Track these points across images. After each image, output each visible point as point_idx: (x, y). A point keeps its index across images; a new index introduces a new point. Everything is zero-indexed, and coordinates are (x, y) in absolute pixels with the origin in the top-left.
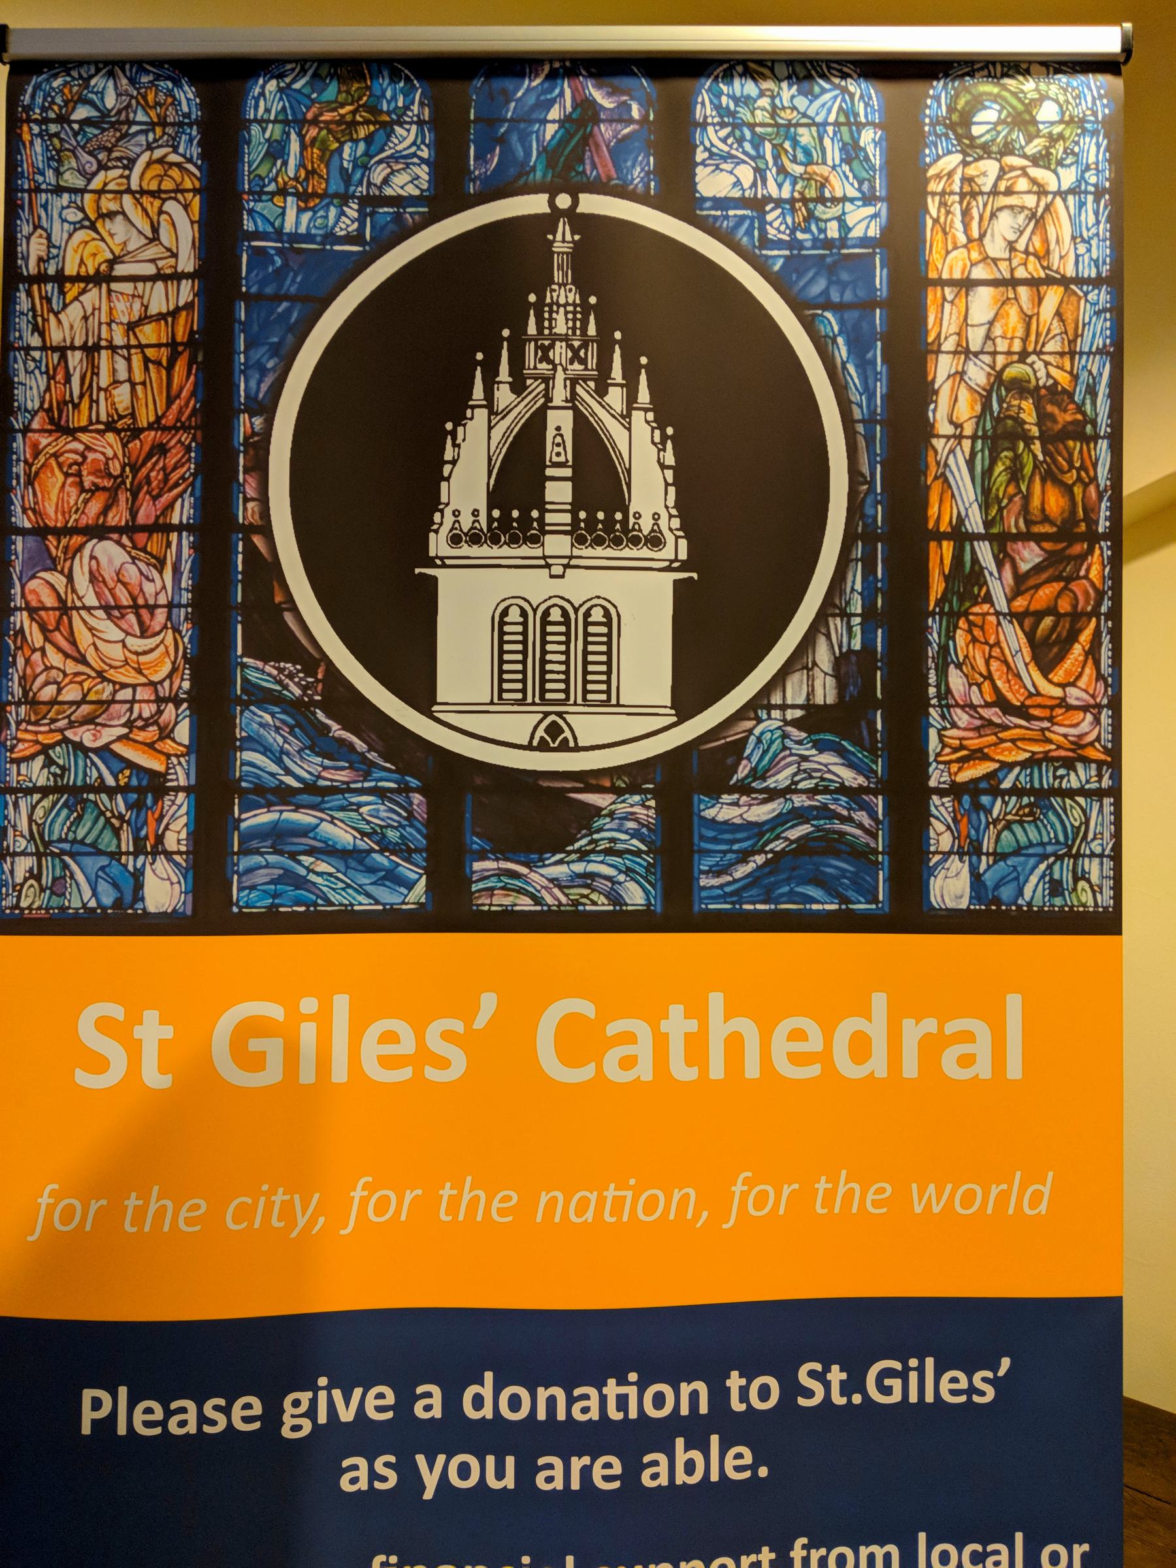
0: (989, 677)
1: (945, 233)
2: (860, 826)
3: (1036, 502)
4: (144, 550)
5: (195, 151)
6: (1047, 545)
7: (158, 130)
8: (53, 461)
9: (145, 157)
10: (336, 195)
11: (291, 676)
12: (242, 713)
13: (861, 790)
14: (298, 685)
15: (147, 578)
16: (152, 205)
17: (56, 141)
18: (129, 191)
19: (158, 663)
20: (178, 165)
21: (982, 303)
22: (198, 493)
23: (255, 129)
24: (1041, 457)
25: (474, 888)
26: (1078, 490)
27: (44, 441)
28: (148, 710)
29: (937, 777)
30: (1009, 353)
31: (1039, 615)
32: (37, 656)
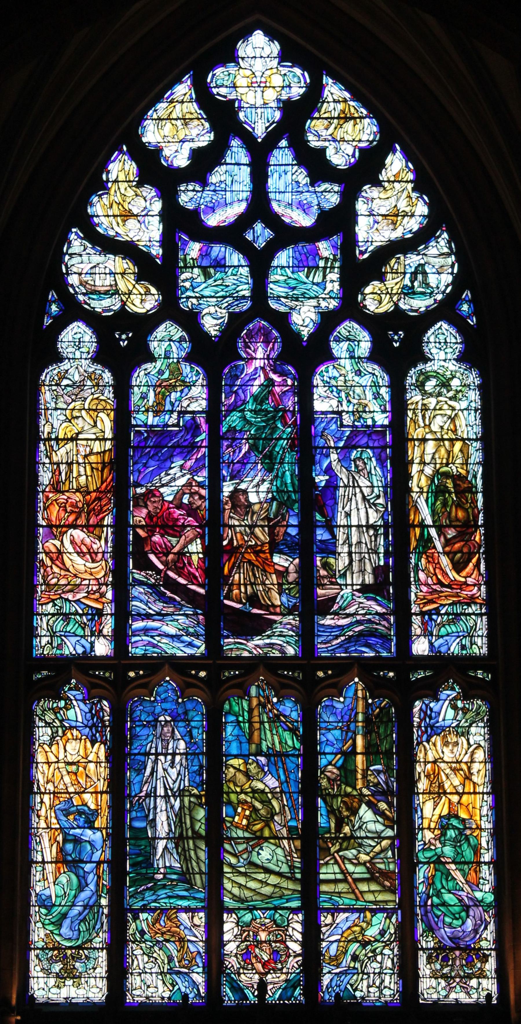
0: (435, 574)
1: (415, 423)
2: (384, 626)
3: (453, 514)
4: (93, 533)
5: (111, 396)
6: (458, 529)
7: (96, 388)
8: (54, 503)
9: (91, 397)
10: (168, 411)
11: (151, 576)
13: (384, 613)
16: (94, 414)
17: (55, 392)
18: (84, 409)
19: (98, 573)
20: (104, 400)
21: (430, 447)
22: (114, 514)
23: (136, 389)
24: (455, 499)
25: (225, 648)
27: (51, 495)
28: (95, 588)
29: (415, 609)
30: (441, 463)
31: (455, 553)
32: (49, 569)
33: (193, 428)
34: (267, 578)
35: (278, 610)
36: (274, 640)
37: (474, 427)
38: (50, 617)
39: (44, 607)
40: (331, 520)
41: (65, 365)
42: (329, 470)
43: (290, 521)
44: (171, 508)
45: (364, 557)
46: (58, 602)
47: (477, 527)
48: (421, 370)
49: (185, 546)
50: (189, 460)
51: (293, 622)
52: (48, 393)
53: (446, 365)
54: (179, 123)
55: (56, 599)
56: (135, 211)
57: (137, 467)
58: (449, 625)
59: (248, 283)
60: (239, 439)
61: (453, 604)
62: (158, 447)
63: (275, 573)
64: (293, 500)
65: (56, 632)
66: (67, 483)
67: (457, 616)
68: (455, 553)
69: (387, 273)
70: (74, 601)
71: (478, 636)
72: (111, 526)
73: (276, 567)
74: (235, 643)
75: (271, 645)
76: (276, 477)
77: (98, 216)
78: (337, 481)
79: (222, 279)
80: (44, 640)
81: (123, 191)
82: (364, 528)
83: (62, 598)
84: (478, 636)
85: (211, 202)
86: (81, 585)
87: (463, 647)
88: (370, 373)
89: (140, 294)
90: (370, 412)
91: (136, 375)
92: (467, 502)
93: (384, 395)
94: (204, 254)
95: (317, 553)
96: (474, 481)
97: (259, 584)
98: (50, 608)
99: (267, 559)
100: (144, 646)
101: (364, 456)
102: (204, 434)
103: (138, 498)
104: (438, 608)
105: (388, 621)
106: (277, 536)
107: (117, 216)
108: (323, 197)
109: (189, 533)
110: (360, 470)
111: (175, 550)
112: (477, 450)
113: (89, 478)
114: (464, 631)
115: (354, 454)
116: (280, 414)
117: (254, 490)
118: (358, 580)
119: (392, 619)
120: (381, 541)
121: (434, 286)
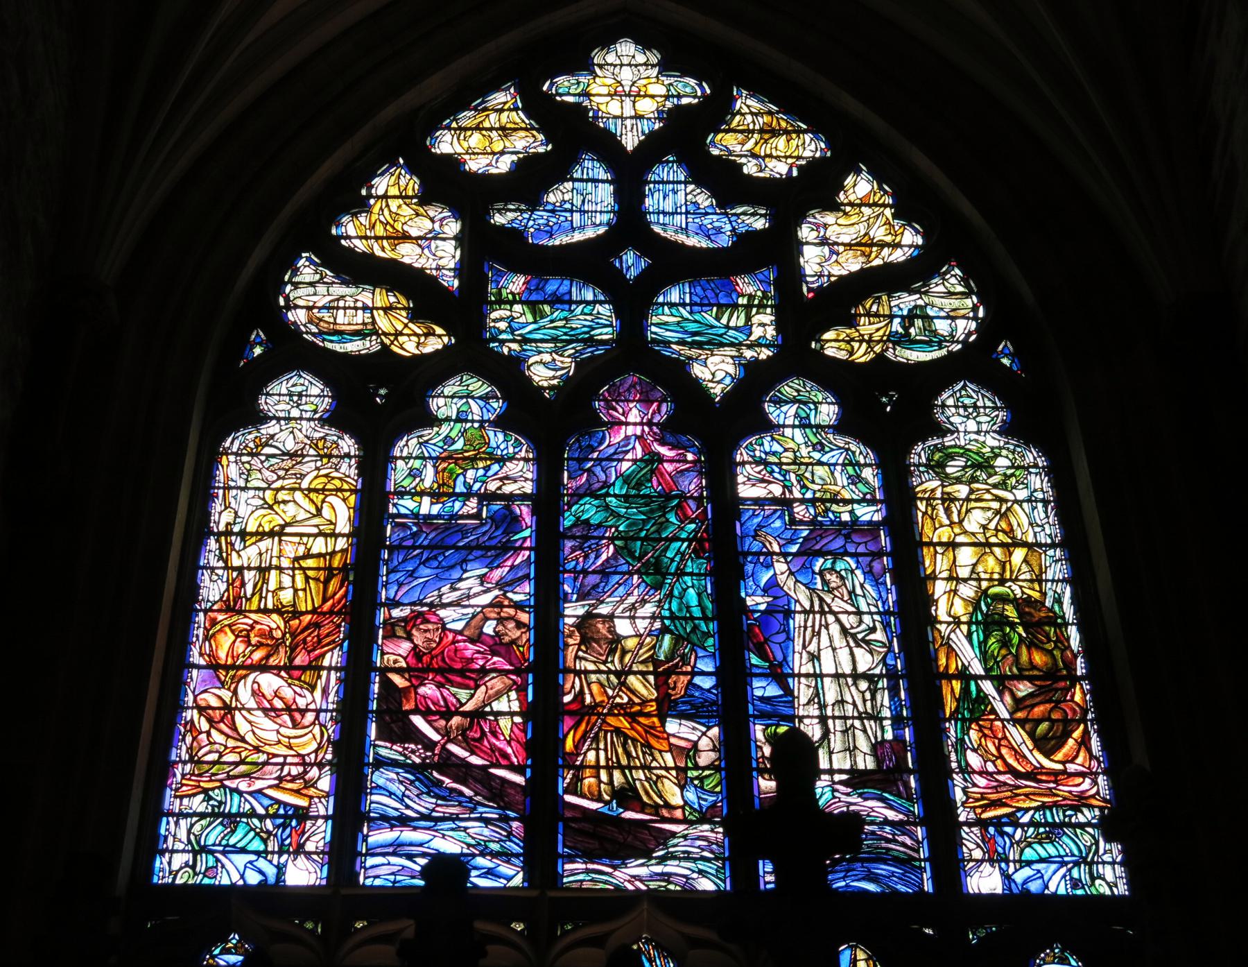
0: (1001, 757)
4: (299, 679)
5: (353, 472)
6: (1038, 683)
8: (227, 629)
11: (413, 752)
12: (372, 773)
13: (901, 823)
14: (419, 757)
15: (300, 695)
16: (318, 498)
17: (247, 466)
18: (300, 489)
20: (340, 479)
21: (966, 556)
22: (345, 648)
23: (400, 463)
24: (1024, 635)
25: (565, 880)
26: (1057, 653)
28: (295, 771)
30: (991, 580)
32: (203, 736)
34: (654, 759)
35: (678, 814)
36: (672, 867)
37: (1047, 526)
38: (195, 819)
39: (185, 801)
40: (781, 665)
41: (271, 428)
42: (772, 586)
43: (698, 665)
44: (459, 641)
45: (852, 725)
46: (217, 794)
47: (1075, 680)
48: (935, 446)
50: (497, 567)
52: (233, 466)
53: (981, 439)
54: (494, 134)
55: (213, 789)
56: (414, 233)
57: (394, 577)
58: (1040, 843)
59: (611, 326)
60: (594, 538)
61: (1043, 807)
62: (437, 547)
63: (670, 751)
64: (703, 632)
65: (205, 846)
66: (256, 598)
68: (1038, 722)
69: (860, 315)
70: (250, 793)
71: (1104, 863)
72: (337, 669)
73: (672, 740)
74: (588, 871)
75: (667, 877)
76: (670, 595)
77: (348, 237)
78: (789, 604)
79: (566, 319)
80: (178, 860)
81: (394, 209)
82: (850, 680)
83: (225, 787)
84: (1104, 863)
85: (547, 225)
86: (266, 763)
87: (1076, 883)
88: (840, 448)
89: (415, 334)
91: (402, 443)
92: (1049, 640)
93: (870, 478)
95: (755, 717)
96: (1056, 608)
97: (636, 768)
99: (653, 727)
100: (393, 874)
102: (529, 530)
103: (393, 625)
104: (1013, 814)
106: (674, 689)
107: (382, 238)
108: (739, 221)
110: (833, 589)
111: (468, 708)
112: (1056, 561)
113: (301, 594)
114: (1073, 855)
115: (819, 564)
116: (676, 502)
117: (627, 614)
118: (841, 762)
119: (920, 832)
120: (884, 698)
121: (946, 334)
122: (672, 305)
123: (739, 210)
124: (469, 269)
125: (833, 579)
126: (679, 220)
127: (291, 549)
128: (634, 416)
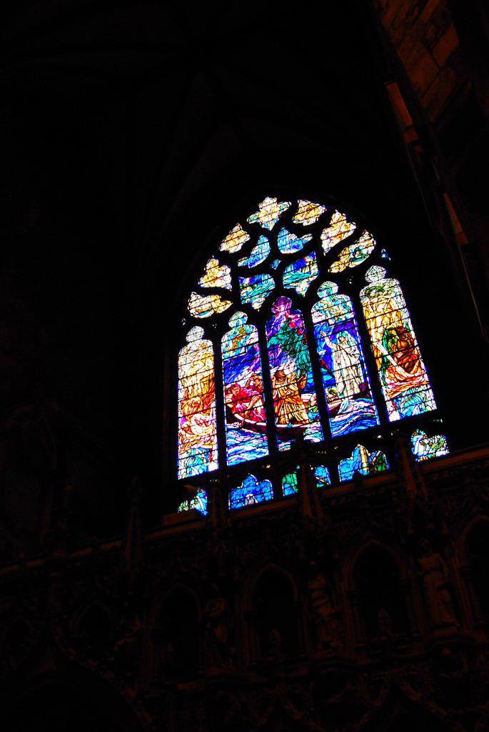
0: (395, 377)
3: (399, 345)
5: (212, 350)
13: (369, 406)
21: (379, 319)
29: (386, 398)
33: (253, 351)
35: (307, 422)
41: (189, 346)
42: (326, 347)
46: (189, 451)
47: (414, 347)
49: (254, 405)
51: (317, 426)
54: (236, 239)
67: (413, 395)
68: (405, 364)
76: (298, 359)
90: (343, 315)
94: (251, 281)
98: (185, 455)
101: (344, 334)
105: (372, 409)
109: (255, 398)
115: (338, 336)
118: (351, 393)
119: (374, 407)
120: (360, 370)
122: (288, 272)
123: (303, 237)
124: (235, 282)
125: (342, 339)
126: (288, 246)
127: (199, 377)
128: (283, 309)
